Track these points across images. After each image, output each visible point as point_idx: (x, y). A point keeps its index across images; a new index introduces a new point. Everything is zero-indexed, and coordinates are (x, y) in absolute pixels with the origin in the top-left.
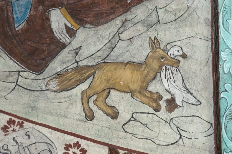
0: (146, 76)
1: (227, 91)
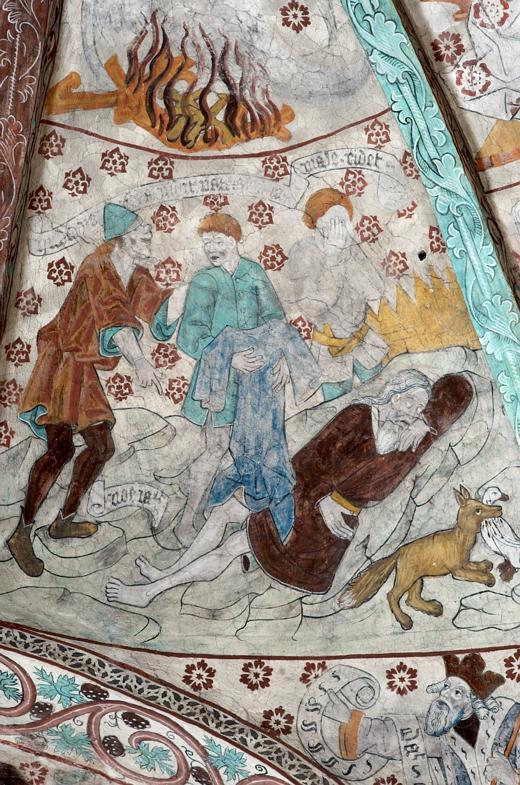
0: (464, 544)
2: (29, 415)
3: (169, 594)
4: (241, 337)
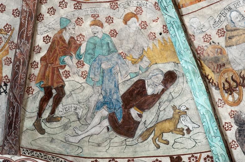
0: (175, 123)
1: (204, 122)
2: (38, 84)
3: (84, 139)
4: (104, 58)
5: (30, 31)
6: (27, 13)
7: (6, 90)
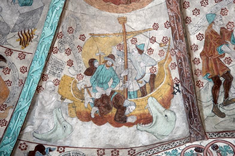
2: (205, 77)
5: (181, 30)
6: (173, 18)
7: (179, 89)
